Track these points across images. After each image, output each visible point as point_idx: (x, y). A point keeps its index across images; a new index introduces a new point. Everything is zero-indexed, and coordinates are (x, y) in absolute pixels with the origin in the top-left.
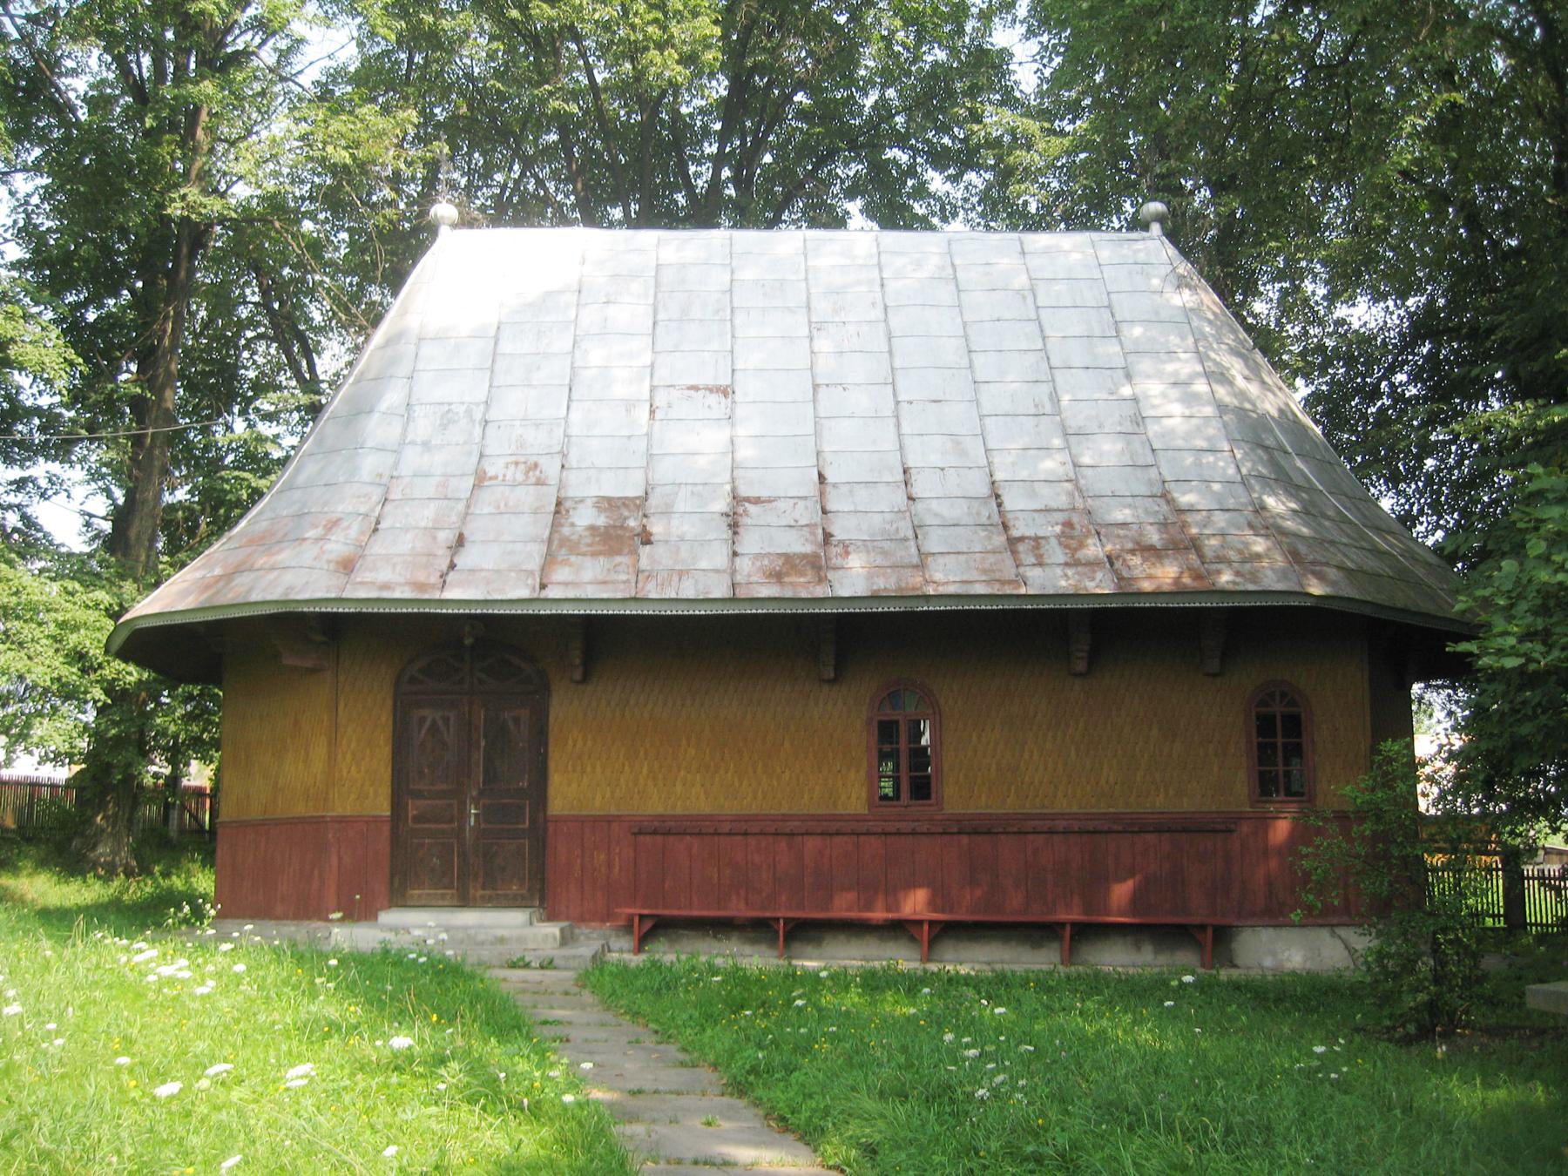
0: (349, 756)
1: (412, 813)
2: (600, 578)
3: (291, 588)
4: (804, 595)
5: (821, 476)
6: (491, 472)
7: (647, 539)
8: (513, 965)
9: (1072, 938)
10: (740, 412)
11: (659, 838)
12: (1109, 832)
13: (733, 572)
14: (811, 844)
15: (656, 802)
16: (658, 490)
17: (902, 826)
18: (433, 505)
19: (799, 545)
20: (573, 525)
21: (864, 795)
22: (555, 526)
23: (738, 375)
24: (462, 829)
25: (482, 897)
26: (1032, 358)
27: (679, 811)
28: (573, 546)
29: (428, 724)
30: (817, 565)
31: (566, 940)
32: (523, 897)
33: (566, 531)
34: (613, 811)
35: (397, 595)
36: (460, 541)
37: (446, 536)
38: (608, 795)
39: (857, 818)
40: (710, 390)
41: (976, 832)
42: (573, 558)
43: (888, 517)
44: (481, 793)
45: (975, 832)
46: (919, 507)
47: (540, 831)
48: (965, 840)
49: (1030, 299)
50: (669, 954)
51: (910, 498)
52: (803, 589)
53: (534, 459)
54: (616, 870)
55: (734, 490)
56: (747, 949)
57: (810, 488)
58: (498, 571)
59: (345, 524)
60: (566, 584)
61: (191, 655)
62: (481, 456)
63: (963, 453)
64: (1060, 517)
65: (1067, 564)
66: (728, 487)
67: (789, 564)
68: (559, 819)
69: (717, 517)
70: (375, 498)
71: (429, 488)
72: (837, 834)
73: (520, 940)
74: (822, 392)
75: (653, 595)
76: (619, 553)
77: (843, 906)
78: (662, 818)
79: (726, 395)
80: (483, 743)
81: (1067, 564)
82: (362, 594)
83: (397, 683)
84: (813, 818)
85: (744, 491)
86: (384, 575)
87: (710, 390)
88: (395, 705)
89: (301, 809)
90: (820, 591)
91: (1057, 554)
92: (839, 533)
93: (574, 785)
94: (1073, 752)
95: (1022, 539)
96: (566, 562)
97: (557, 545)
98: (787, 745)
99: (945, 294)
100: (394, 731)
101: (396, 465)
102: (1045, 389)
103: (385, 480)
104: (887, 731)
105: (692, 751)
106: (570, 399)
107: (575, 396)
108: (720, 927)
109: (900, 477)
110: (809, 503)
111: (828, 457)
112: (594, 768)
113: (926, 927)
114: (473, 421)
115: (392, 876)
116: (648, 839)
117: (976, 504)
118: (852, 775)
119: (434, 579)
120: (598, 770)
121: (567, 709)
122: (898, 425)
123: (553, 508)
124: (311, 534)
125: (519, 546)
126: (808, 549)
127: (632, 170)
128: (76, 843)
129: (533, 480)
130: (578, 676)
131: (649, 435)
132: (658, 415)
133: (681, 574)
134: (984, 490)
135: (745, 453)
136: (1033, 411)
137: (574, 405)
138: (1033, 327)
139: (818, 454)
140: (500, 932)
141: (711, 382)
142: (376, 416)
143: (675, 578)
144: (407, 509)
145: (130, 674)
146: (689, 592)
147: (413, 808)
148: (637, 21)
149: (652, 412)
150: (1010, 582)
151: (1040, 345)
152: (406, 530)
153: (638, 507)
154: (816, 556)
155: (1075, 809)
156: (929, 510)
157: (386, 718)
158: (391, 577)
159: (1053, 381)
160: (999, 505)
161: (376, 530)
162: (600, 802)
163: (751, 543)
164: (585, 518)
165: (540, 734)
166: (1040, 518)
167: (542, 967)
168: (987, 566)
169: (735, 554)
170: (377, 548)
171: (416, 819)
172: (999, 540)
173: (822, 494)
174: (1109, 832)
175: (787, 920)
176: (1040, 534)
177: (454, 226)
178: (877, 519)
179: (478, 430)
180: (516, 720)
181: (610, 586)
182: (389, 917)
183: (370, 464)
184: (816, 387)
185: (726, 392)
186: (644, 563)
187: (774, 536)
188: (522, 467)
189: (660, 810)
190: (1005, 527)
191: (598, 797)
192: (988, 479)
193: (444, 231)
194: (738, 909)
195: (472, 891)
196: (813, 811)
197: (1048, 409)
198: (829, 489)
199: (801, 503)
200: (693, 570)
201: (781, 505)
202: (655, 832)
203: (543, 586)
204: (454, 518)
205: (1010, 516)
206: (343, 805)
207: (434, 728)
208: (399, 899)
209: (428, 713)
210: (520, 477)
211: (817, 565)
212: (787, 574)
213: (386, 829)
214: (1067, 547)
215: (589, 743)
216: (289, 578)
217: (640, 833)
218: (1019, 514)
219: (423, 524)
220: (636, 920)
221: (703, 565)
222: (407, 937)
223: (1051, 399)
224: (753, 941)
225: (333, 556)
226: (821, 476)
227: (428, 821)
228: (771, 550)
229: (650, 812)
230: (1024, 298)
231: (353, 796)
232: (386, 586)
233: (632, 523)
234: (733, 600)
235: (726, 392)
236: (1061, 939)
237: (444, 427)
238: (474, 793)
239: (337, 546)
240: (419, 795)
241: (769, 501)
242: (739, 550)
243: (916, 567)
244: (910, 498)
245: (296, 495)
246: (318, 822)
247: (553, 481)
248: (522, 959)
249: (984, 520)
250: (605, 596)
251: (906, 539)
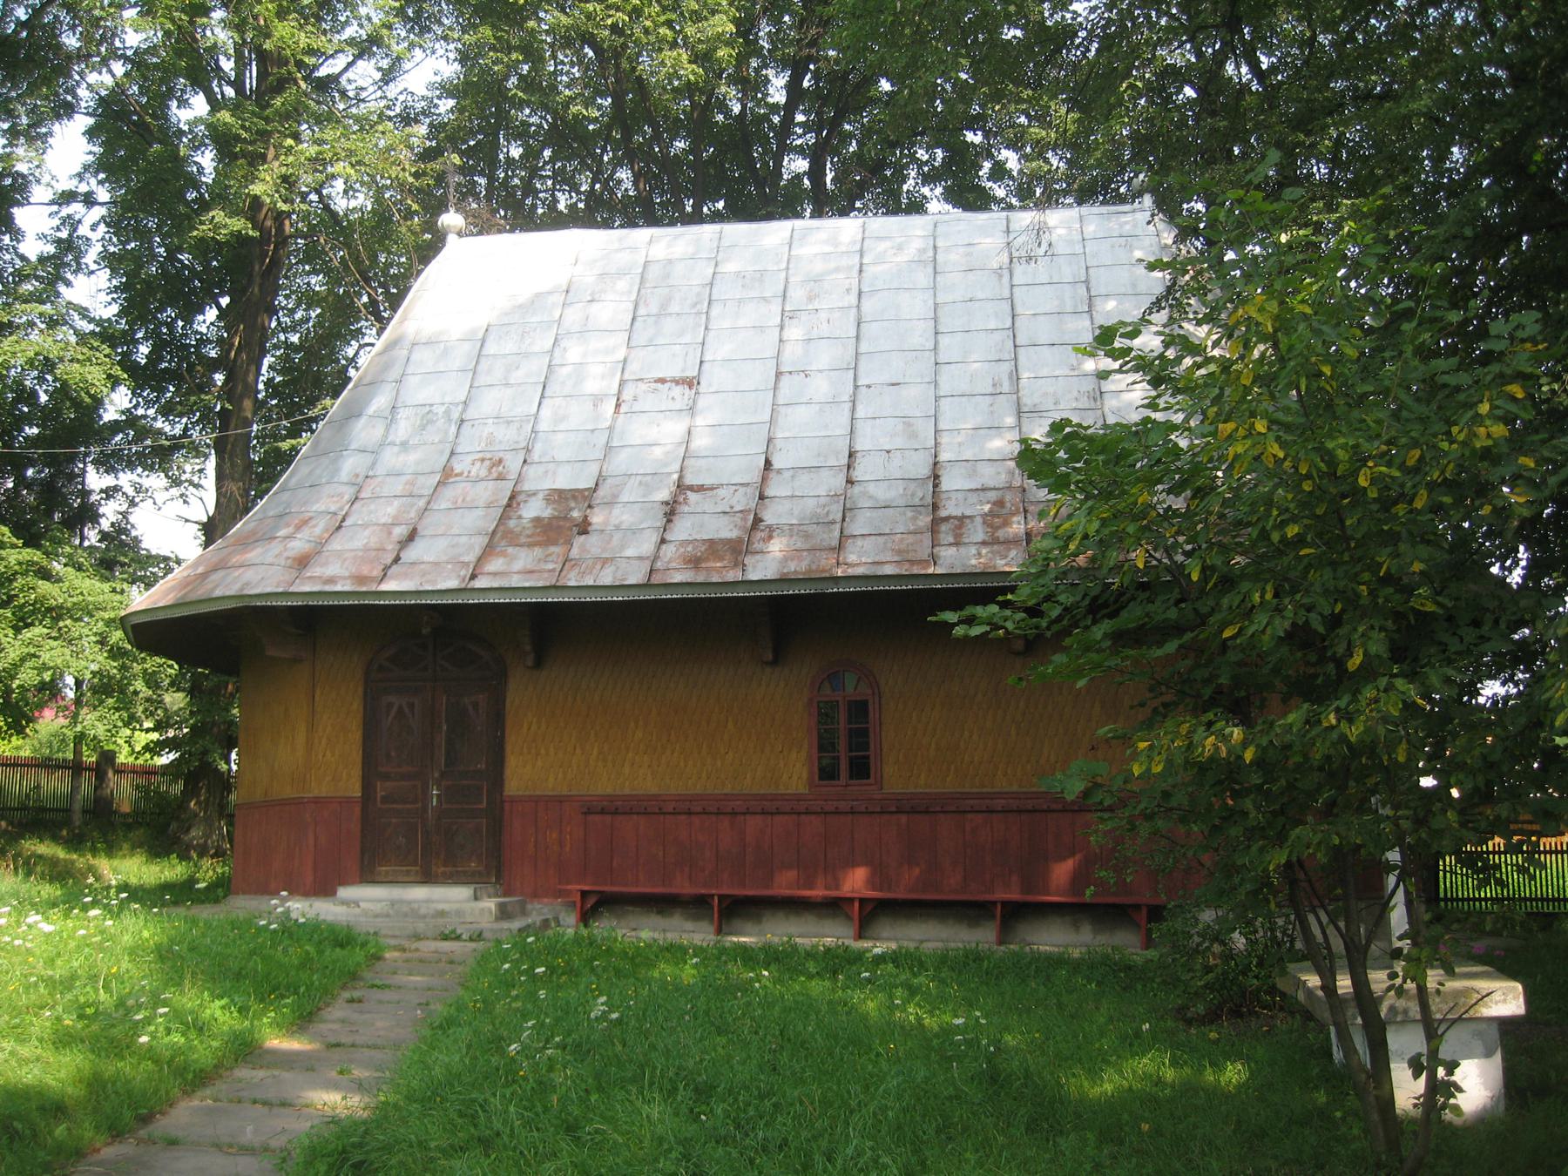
0: (324, 741)
1: (380, 794)
2: (529, 567)
3: (247, 584)
4: (714, 580)
5: (768, 463)
6: (458, 468)
7: (584, 528)
8: (445, 938)
9: (1003, 916)
10: (701, 403)
11: (608, 818)
12: (1049, 811)
13: (656, 558)
14: (753, 824)
15: (604, 784)
16: (609, 481)
17: (843, 805)
18: (396, 503)
19: (726, 530)
20: (520, 517)
21: (805, 775)
22: (503, 518)
23: (706, 366)
24: (425, 809)
25: (444, 874)
26: (998, 336)
27: (627, 791)
28: (513, 539)
29: (395, 709)
30: (738, 550)
31: (504, 913)
33: (512, 523)
35: (338, 588)
36: (412, 536)
37: (400, 531)
39: (798, 798)
40: (677, 382)
41: (913, 811)
42: (510, 550)
43: (823, 500)
44: (442, 774)
45: (913, 811)
46: (856, 489)
48: (904, 818)
49: (1006, 279)
50: (610, 929)
51: (850, 482)
52: (721, 572)
53: (501, 455)
55: (680, 478)
56: (689, 925)
57: (754, 476)
58: (436, 564)
59: (313, 522)
60: (495, 574)
61: (215, 645)
62: (452, 453)
63: (913, 435)
64: (993, 495)
65: (984, 543)
66: (676, 476)
67: (714, 548)
68: (514, 800)
69: (657, 506)
70: (346, 497)
71: (398, 486)
72: (778, 812)
73: (459, 913)
74: (785, 380)
75: (572, 583)
76: (555, 543)
77: (784, 884)
78: (611, 798)
79: (690, 386)
81: (984, 543)
82: (307, 589)
84: (763, 797)
85: (690, 480)
86: (332, 570)
87: (677, 382)
88: (365, 693)
89: (289, 792)
90: (732, 575)
91: (978, 533)
92: (769, 517)
94: (1013, 732)
95: (947, 519)
96: (503, 554)
97: (499, 538)
98: (730, 725)
99: (923, 277)
101: (374, 464)
102: (1007, 367)
103: (360, 480)
104: (825, 714)
105: (639, 734)
106: (542, 396)
107: (548, 393)
108: (662, 904)
109: (845, 461)
110: (749, 490)
111: (778, 444)
113: (857, 905)
114: (450, 420)
115: (363, 853)
116: (597, 818)
117: (912, 486)
118: (794, 755)
119: (377, 572)
121: (521, 692)
122: (853, 410)
123: (505, 502)
124: (281, 533)
125: (463, 540)
126: (734, 534)
127: (707, 168)
128: (174, 826)
129: (495, 475)
131: (611, 429)
132: (623, 409)
133: (605, 561)
134: (925, 471)
135: (700, 442)
136: (990, 390)
137: (546, 402)
138: (1006, 307)
139: (770, 440)
140: (440, 907)
141: (677, 374)
142: (363, 420)
143: (598, 567)
144: (372, 507)
145: (171, 667)
146: (607, 578)
147: (381, 789)
148: (648, 23)
149: (618, 406)
150: (920, 562)
151: (1008, 324)
152: (365, 526)
153: (585, 498)
154: (739, 540)
155: (1015, 788)
156: (864, 493)
157: (357, 705)
158: (337, 574)
159: (1016, 359)
160: (936, 486)
161: (340, 527)
162: (553, 784)
163: (683, 530)
164: (533, 509)
165: (498, 719)
166: (973, 498)
167: (471, 939)
168: (903, 547)
169: (663, 541)
170: (336, 545)
171: (385, 800)
172: (925, 520)
173: (764, 479)
174: (1049, 811)
175: (720, 896)
176: (968, 513)
177: (460, 234)
178: (811, 503)
179: (453, 429)
180: (476, 705)
181: (535, 575)
182: (344, 892)
183: (350, 465)
184: (779, 374)
185: (690, 383)
186: (575, 553)
187: (705, 522)
188: (487, 463)
189: (609, 791)
190: (935, 507)
191: (551, 779)
192: (931, 461)
193: (452, 239)
194: (683, 886)
196: (755, 791)
197: (1006, 387)
198: (772, 475)
199: (742, 490)
200: (622, 556)
201: (721, 492)
202: (603, 812)
203: (473, 577)
204: (412, 515)
205: (944, 496)
206: (320, 788)
207: (400, 711)
208: (367, 875)
210: (483, 473)
211: (738, 550)
212: (707, 560)
213: (357, 809)
214: (990, 525)
216: (250, 575)
217: (589, 812)
218: (953, 496)
219: (383, 521)
221: (629, 552)
222: (357, 910)
223: (1010, 377)
224: (696, 918)
225: (290, 554)
226: (768, 463)
228: (698, 537)
229: (600, 792)
230: (1001, 276)
231: (328, 779)
232: (331, 580)
233: (575, 514)
234: (646, 586)
235: (690, 383)
236: (993, 917)
237: (423, 428)
239: (299, 545)
240: (386, 777)
241: (712, 488)
242: (668, 537)
243: (833, 549)
244: (850, 482)
245: (285, 496)
246: (298, 802)
247: (514, 476)
248: (454, 931)
249: (917, 501)
250: (527, 585)
251: (833, 522)
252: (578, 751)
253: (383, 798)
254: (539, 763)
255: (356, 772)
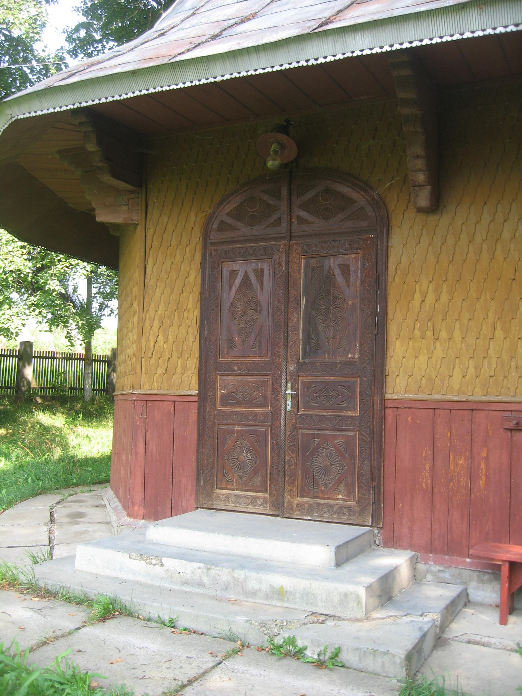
0: (156, 323)
1: (220, 392)
24: (275, 414)
25: (300, 505)
32: (349, 508)
34: (478, 396)
38: (471, 371)
44: (300, 366)
47: (376, 421)
54: (482, 483)
68: (400, 406)
80: (303, 302)
83: (206, 233)
88: (204, 256)
93: (423, 358)
100: (202, 293)
112: (451, 332)
120: (457, 335)
130: (423, 199)
147: (223, 384)
162: (459, 383)
165: (377, 287)
167: (320, 664)
171: (226, 400)
180: (345, 269)
191: (457, 375)
195: (287, 497)
207: (246, 281)
209: (241, 268)
213: (194, 411)
215: (444, 298)
220: (505, 569)
227: (239, 403)
231: (161, 371)
238: (292, 368)
248: (292, 641)
252: (499, 333)
253: (222, 395)
254: (439, 351)
255: (193, 363)
